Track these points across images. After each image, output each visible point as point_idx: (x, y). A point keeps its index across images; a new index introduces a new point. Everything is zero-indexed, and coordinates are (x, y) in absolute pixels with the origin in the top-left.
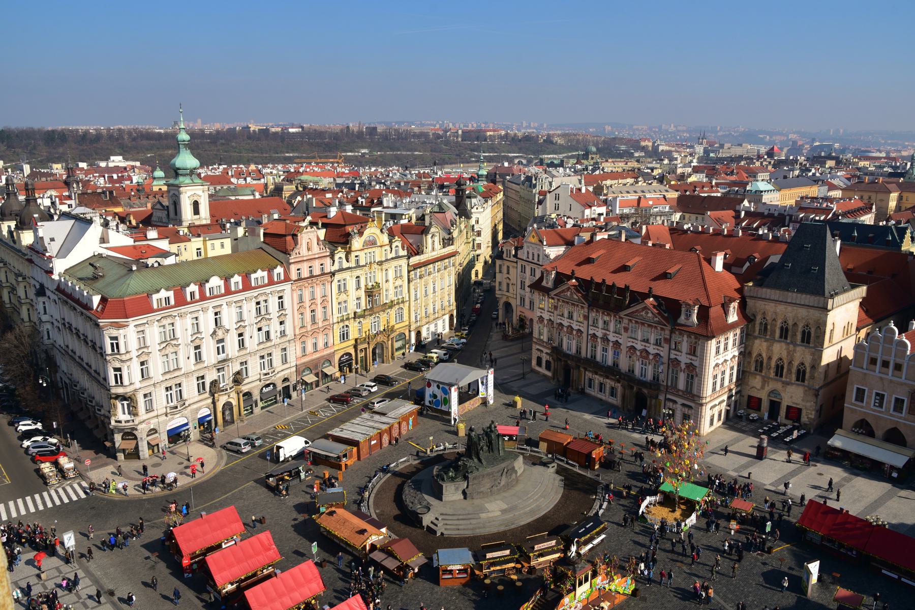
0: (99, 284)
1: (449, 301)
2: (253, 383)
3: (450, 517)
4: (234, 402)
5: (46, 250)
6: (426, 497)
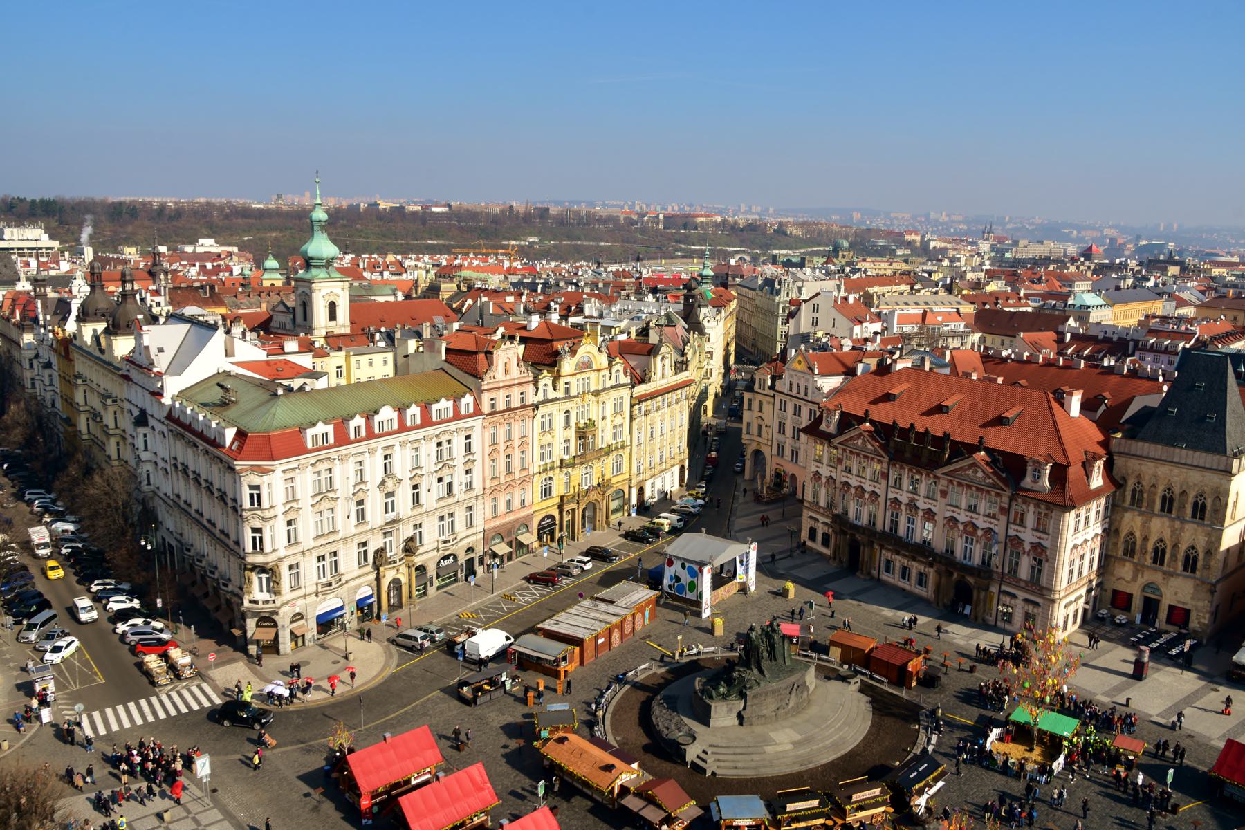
0: (232, 412)
1: (680, 447)
2: (427, 556)
3: (723, 751)
4: (404, 580)
5: (152, 364)
6: (686, 720)
